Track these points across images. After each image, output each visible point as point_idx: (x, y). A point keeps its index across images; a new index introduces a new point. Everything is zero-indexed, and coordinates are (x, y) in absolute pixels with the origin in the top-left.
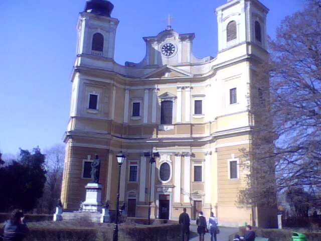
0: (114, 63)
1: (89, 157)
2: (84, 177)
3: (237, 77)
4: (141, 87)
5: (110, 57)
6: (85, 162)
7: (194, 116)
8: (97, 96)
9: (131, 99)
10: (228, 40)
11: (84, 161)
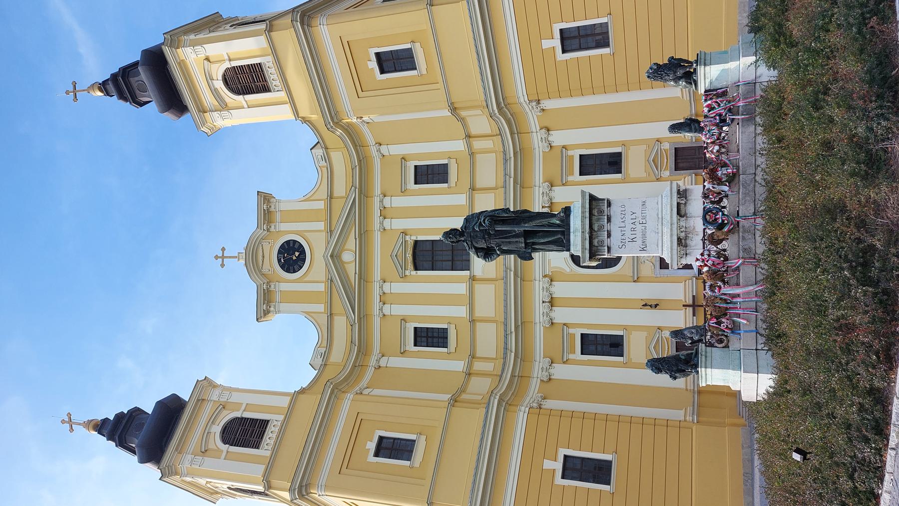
0: (303, 391)
1: (548, 464)
2: (608, 483)
3: (348, 48)
4: (376, 322)
5: (288, 399)
6: (563, 477)
7: (453, 185)
8: (381, 439)
9: (403, 353)
10: (266, 89)
11: (559, 481)
